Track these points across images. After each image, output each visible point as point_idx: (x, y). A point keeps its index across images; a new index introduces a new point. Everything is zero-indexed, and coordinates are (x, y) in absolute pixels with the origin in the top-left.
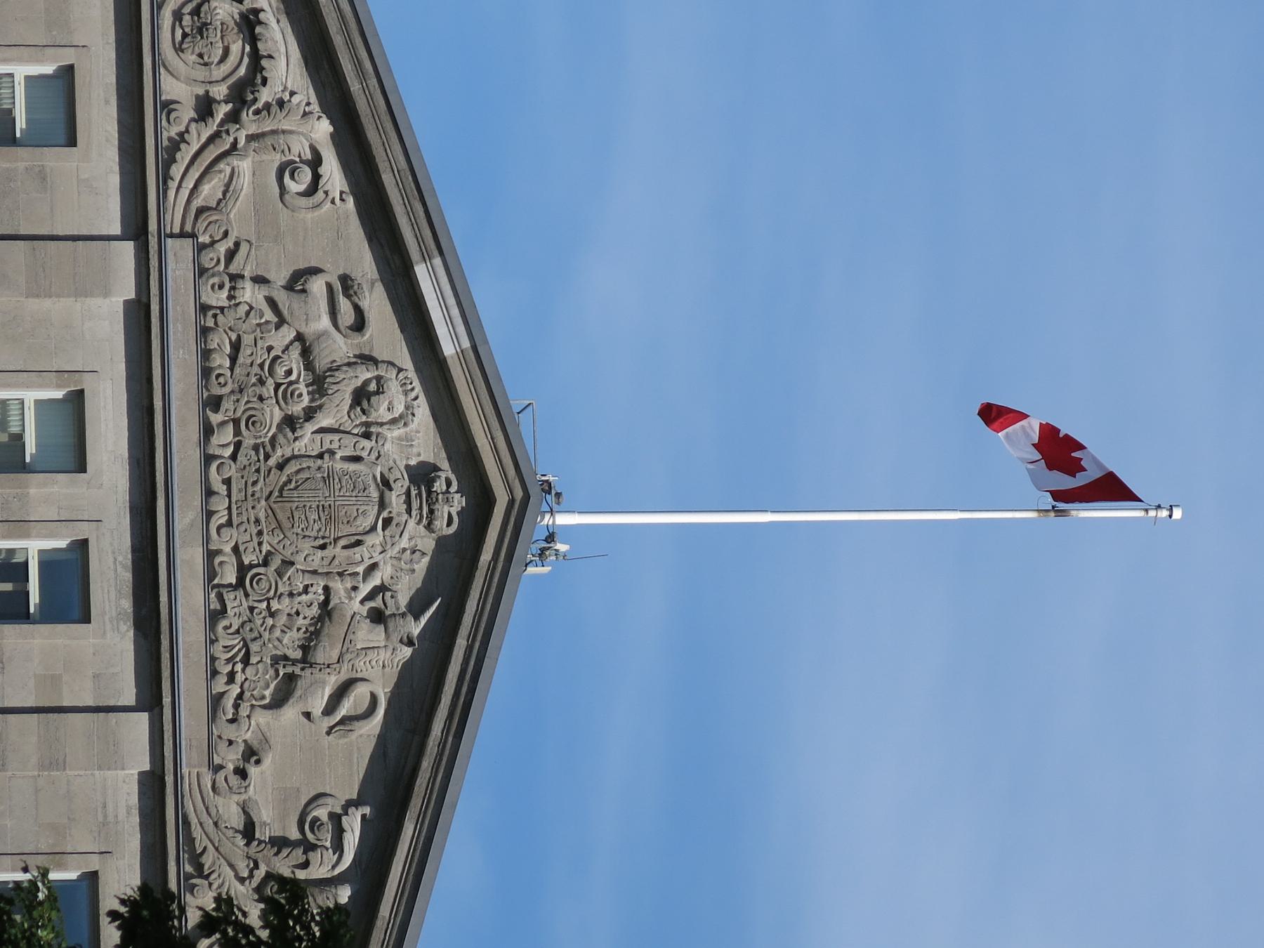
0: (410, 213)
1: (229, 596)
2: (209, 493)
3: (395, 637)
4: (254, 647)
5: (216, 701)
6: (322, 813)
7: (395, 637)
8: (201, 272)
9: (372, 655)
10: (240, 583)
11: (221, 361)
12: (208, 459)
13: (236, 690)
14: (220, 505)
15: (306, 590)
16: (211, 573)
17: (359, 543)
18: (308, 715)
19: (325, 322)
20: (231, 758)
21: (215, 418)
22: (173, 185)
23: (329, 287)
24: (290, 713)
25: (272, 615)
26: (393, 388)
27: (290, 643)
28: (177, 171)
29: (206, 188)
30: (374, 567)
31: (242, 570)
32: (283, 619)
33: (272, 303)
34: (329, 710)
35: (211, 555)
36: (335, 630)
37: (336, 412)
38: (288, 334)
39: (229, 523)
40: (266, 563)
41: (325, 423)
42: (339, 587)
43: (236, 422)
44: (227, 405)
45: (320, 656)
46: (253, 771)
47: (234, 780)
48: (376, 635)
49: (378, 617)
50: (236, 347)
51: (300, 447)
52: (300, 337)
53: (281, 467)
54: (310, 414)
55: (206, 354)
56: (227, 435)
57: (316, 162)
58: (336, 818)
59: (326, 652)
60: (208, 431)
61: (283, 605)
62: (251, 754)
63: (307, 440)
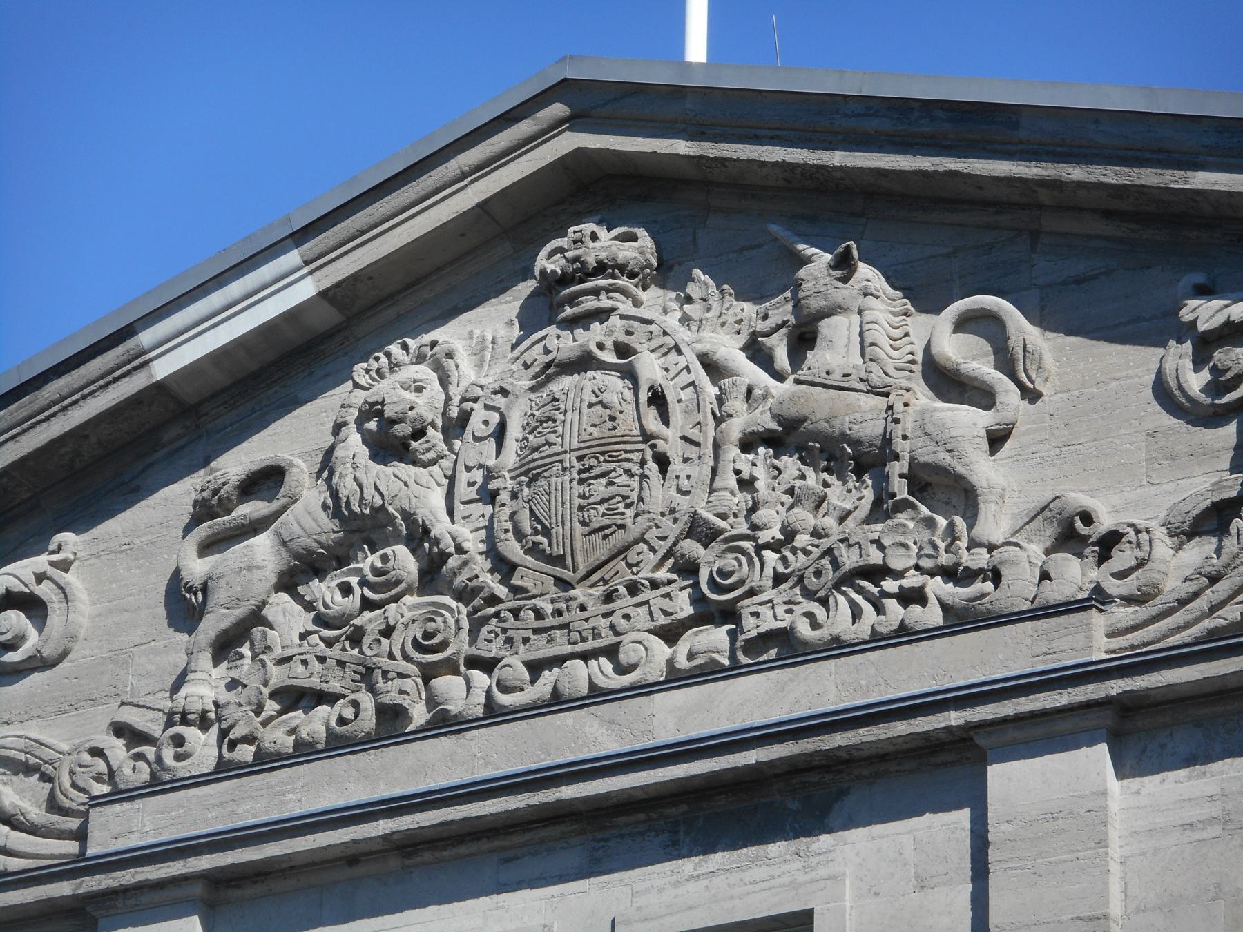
0: (63, 404)
1: (752, 627)
3: (841, 293)
4: (850, 558)
5: (960, 620)
6: (1196, 382)
7: (841, 293)
8: (159, 784)
9: (878, 334)
10: (729, 614)
11: (315, 723)
12: (493, 713)
13: (937, 587)
14: (578, 675)
15: (747, 484)
16: (708, 672)
17: (658, 399)
18: (996, 439)
19: (263, 543)
20: (1074, 574)
21: (419, 714)
23: (208, 547)
24: (983, 470)
25: (789, 534)
27: (849, 494)
30: (714, 368)
31: (707, 614)
32: (804, 517)
33: (224, 647)
34: (983, 396)
35: (675, 678)
36: (821, 407)
37: (419, 490)
38: (283, 609)
39: (611, 652)
40: (688, 569)
41: (437, 499)
43: (429, 673)
44: (391, 692)
45: (871, 429)
46: (1106, 522)
47: (1122, 558)
48: (838, 334)
49: (804, 339)
50: (295, 698)
51: (474, 543)
52: (288, 582)
53: (504, 567)
54: (418, 535)
55: (304, 751)
56: (450, 687)
58: (1206, 345)
59: (862, 417)
60: (444, 723)
61: (772, 521)
62: (1072, 533)
63: (462, 532)
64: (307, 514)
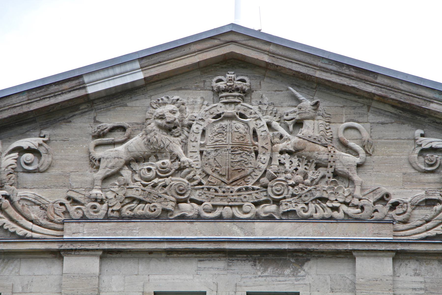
2: (220, 218)
11: (139, 209)
12: (199, 218)
16: (270, 218)
22: (29, 234)
26: (159, 111)
28: (21, 232)
29: (33, 216)
35: (257, 218)
42: (281, 146)
47: (399, 210)
52: (128, 164)
57: (21, 150)
64: (137, 143)
